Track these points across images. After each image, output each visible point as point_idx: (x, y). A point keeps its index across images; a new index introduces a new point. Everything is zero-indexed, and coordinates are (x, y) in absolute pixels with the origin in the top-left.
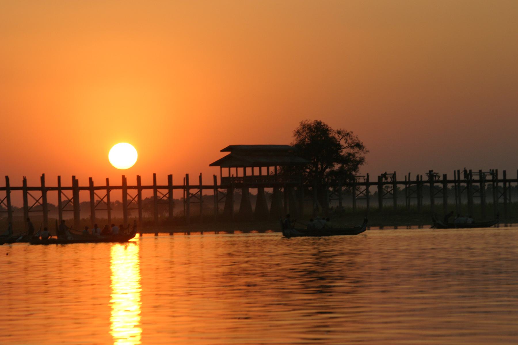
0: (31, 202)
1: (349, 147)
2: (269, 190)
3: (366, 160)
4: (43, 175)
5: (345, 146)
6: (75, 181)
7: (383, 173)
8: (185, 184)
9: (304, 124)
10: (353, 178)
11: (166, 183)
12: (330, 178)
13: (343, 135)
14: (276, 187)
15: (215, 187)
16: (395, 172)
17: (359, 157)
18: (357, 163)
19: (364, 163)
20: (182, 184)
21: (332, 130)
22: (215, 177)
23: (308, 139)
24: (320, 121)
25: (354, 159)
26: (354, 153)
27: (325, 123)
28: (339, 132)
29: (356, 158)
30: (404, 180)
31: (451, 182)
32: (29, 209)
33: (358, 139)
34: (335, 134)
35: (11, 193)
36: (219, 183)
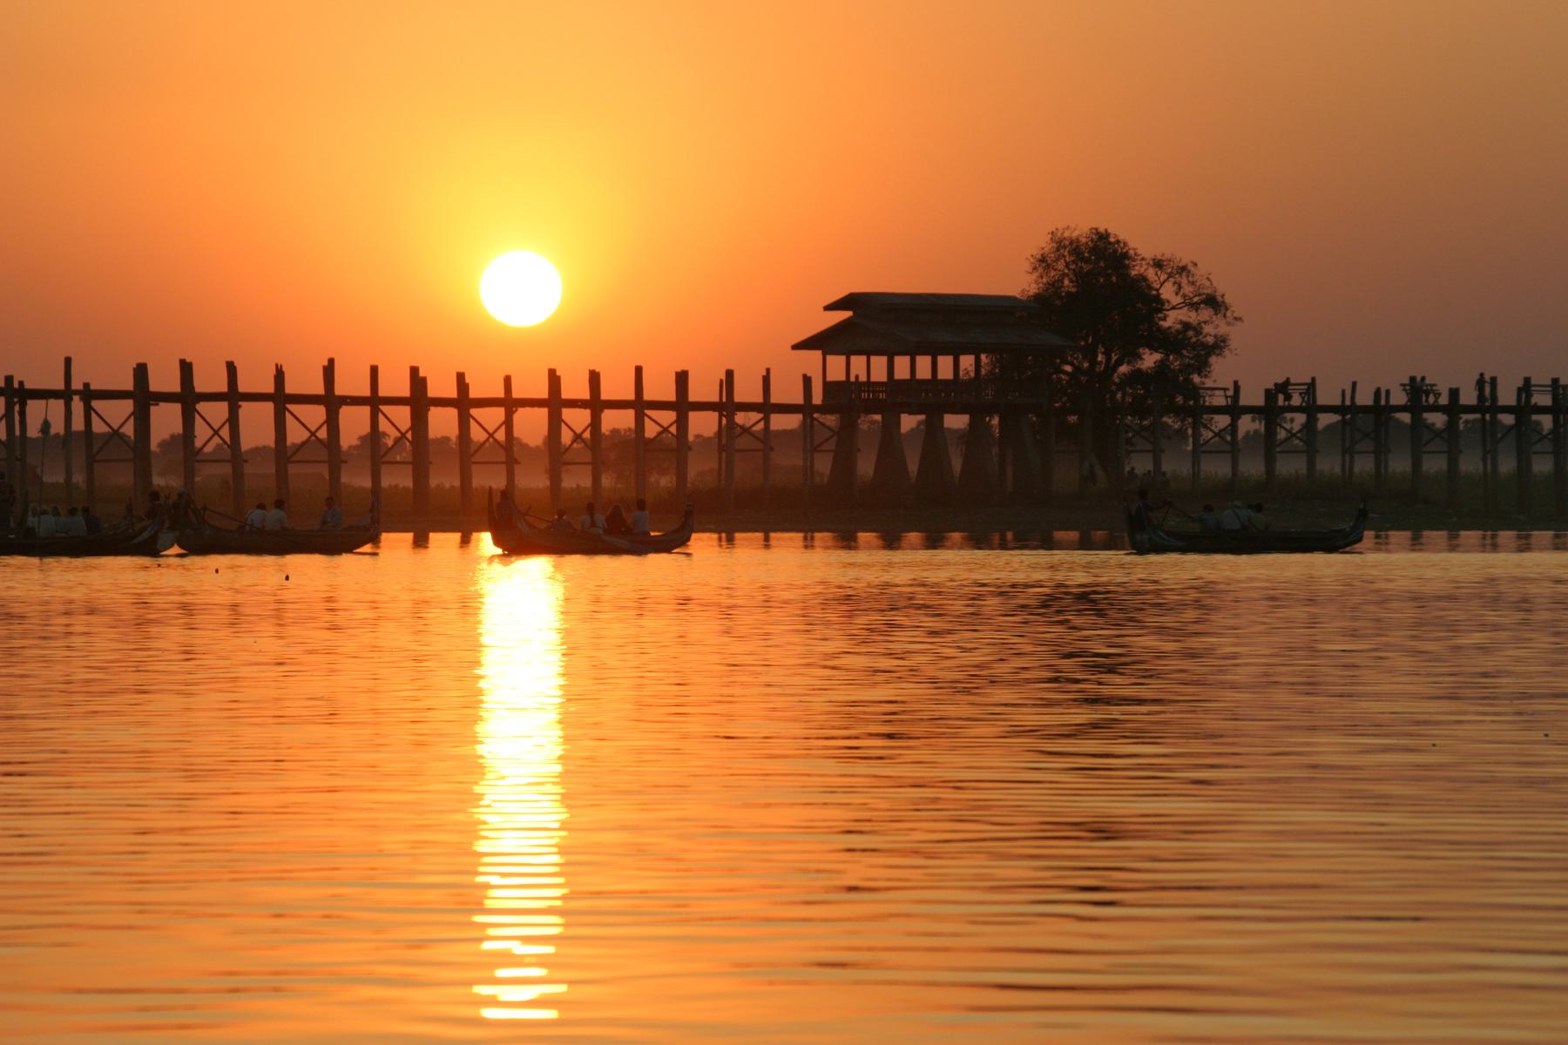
0: (295, 435)
2: (956, 422)
3: (1234, 342)
4: (331, 361)
5: (1175, 304)
6: (417, 381)
8: (724, 400)
10: (1194, 392)
11: (671, 396)
12: (1130, 391)
13: (1169, 270)
14: (977, 412)
15: (806, 409)
16: (1313, 379)
17: (1213, 334)
18: (1205, 351)
19: (1227, 352)
20: (715, 399)
21: (1139, 255)
22: (807, 381)
23: (1071, 281)
25: (1198, 341)
26: (1199, 324)
28: (1158, 264)
29: (1205, 336)
30: (1337, 402)
31: (1469, 409)
32: (289, 454)
35: (241, 411)
36: (817, 399)
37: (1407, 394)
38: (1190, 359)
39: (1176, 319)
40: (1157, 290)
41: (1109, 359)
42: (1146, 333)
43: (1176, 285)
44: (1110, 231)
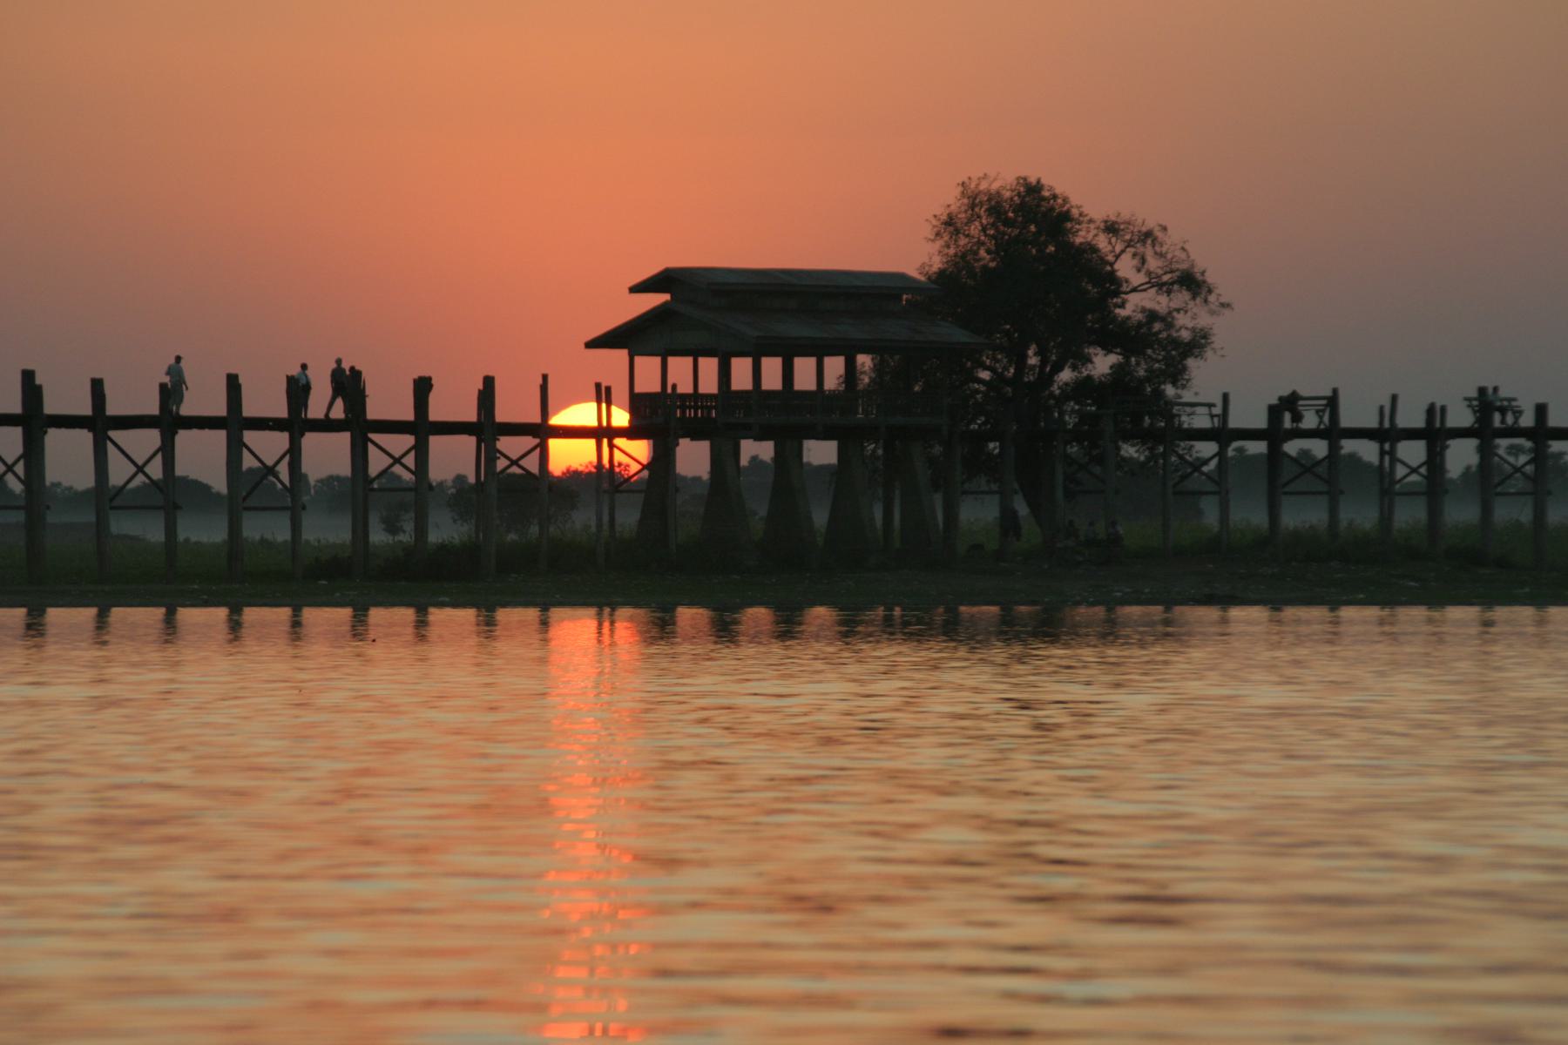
1: (1151, 287)
3: (1218, 340)
7: (1286, 392)
9: (973, 192)
10: (1166, 410)
13: (1128, 237)
16: (1335, 391)
17: (1190, 325)
19: (1209, 354)
21: (1086, 215)
23: (988, 252)
24: (1038, 182)
25: (1169, 336)
26: (1170, 313)
27: (1058, 191)
28: (1111, 228)
29: (1178, 331)
30: (1373, 423)
33: (1189, 257)
34: (1096, 235)
37: (1475, 412)
38: (1158, 361)
39: (1137, 306)
40: (1112, 265)
41: (1044, 362)
42: (1097, 326)
43: (1138, 257)
44: (1043, 181)
